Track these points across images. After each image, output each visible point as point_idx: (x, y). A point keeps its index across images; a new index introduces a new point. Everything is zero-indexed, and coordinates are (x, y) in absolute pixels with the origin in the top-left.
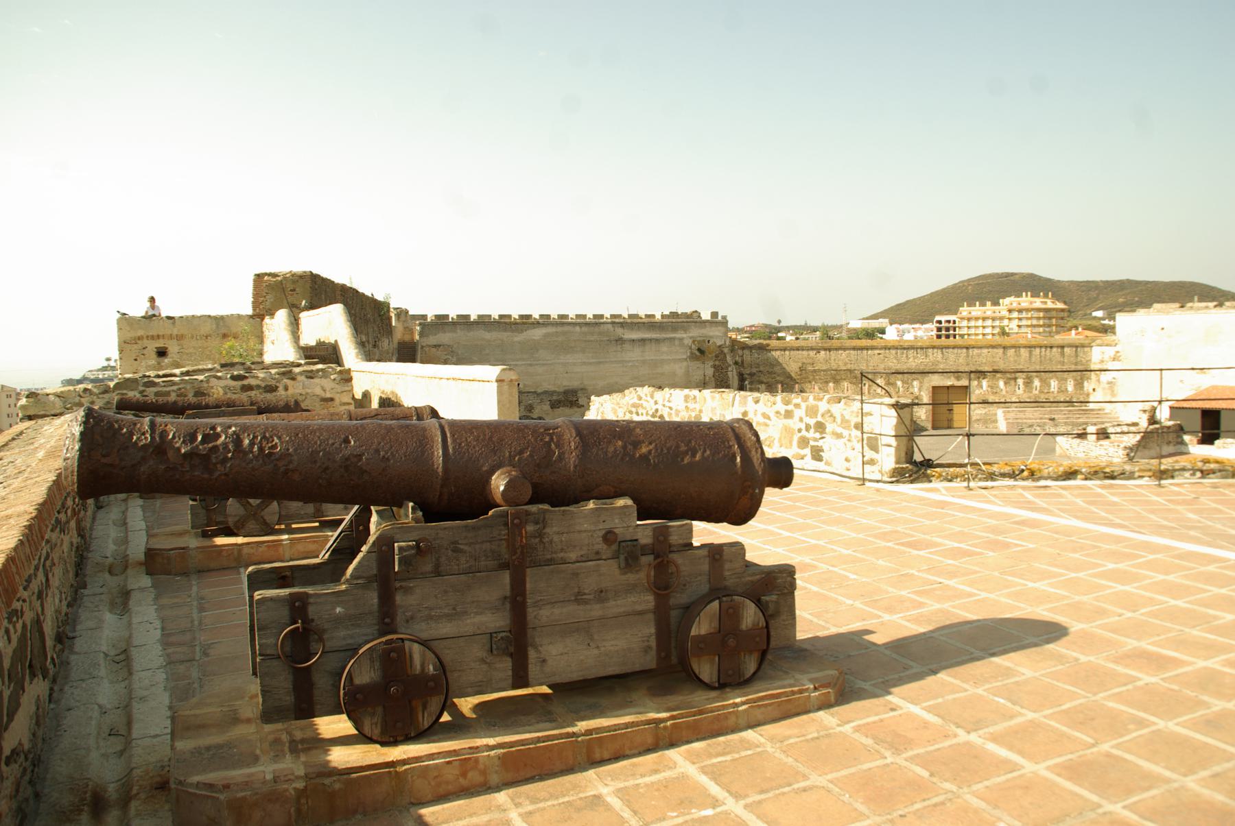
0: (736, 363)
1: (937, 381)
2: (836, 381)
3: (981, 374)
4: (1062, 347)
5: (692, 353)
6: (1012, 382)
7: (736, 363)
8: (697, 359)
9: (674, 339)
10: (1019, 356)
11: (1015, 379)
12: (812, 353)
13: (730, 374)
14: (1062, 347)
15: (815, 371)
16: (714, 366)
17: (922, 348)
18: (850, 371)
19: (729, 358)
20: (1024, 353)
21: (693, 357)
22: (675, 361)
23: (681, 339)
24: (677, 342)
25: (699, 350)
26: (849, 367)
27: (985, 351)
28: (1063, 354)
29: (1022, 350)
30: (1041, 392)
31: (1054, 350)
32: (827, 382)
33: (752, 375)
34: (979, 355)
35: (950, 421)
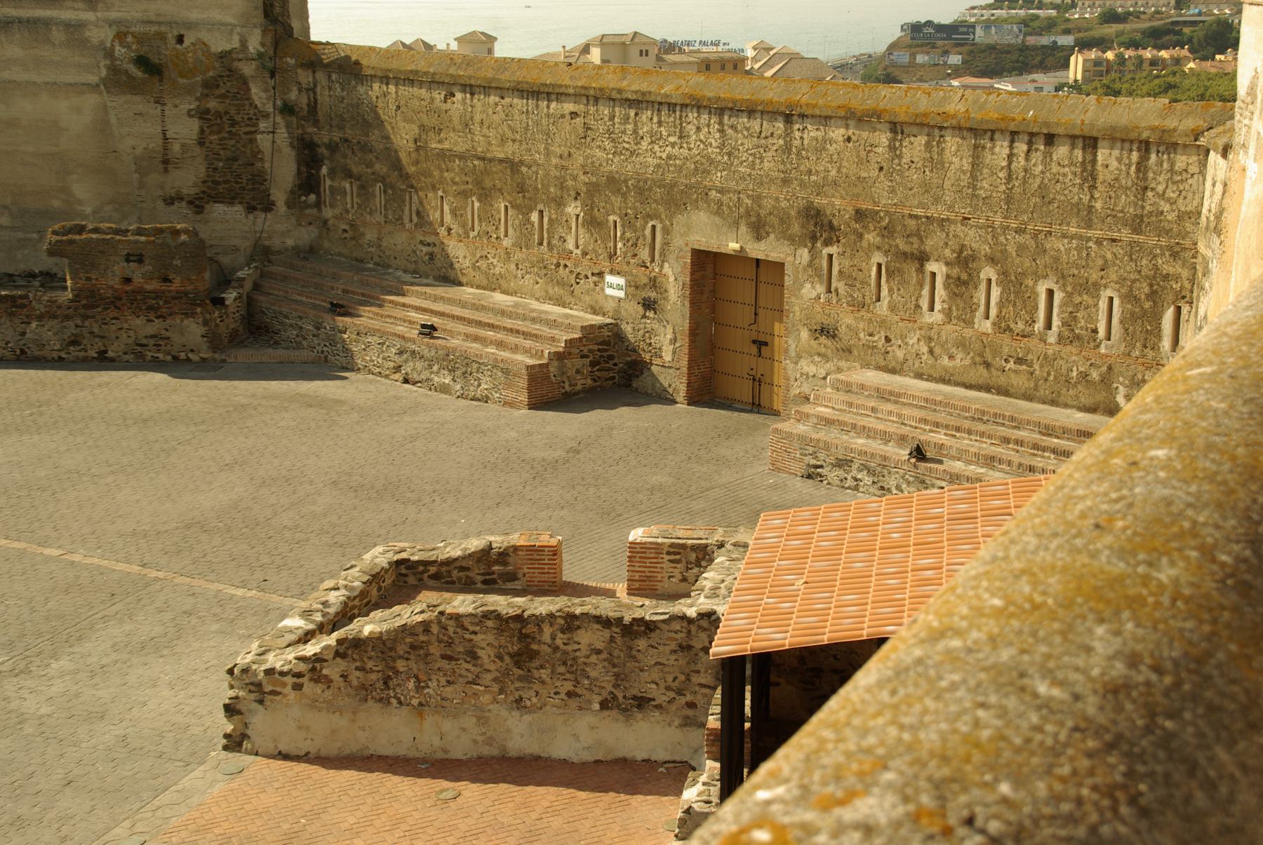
0: (288, 109)
1: (704, 231)
2: (485, 196)
3: (819, 227)
4: (1091, 143)
5: (114, 70)
6: (911, 269)
7: (288, 109)
8: (132, 87)
9: (47, 23)
10: (936, 163)
11: (922, 258)
12: (438, 95)
13: (263, 141)
14: (1091, 143)
15: (442, 154)
16: (203, 114)
17: (672, 107)
18: (513, 165)
19: (258, 94)
20: (955, 150)
21: (116, 81)
22: (54, 88)
23: (74, 28)
24: (58, 35)
25: (142, 61)
26: (510, 150)
27: (838, 133)
28: (1089, 175)
29: (952, 143)
30: (1002, 327)
31: (1061, 151)
32: (465, 194)
33: (333, 147)
34: (821, 147)
35: (758, 382)
